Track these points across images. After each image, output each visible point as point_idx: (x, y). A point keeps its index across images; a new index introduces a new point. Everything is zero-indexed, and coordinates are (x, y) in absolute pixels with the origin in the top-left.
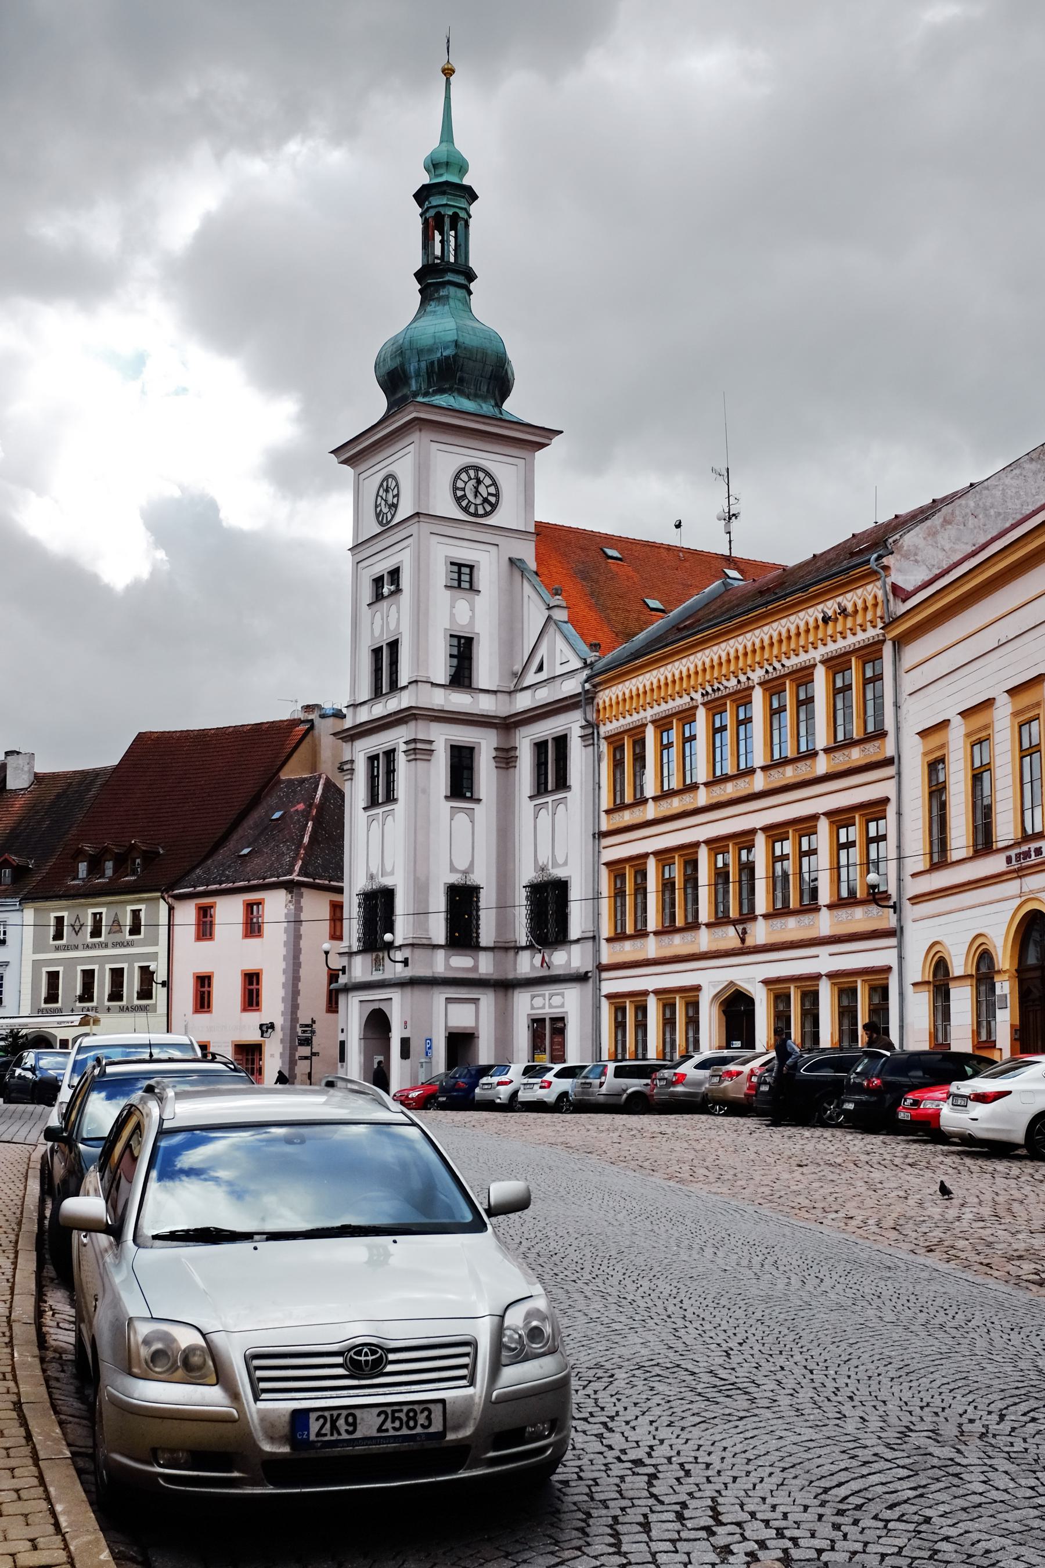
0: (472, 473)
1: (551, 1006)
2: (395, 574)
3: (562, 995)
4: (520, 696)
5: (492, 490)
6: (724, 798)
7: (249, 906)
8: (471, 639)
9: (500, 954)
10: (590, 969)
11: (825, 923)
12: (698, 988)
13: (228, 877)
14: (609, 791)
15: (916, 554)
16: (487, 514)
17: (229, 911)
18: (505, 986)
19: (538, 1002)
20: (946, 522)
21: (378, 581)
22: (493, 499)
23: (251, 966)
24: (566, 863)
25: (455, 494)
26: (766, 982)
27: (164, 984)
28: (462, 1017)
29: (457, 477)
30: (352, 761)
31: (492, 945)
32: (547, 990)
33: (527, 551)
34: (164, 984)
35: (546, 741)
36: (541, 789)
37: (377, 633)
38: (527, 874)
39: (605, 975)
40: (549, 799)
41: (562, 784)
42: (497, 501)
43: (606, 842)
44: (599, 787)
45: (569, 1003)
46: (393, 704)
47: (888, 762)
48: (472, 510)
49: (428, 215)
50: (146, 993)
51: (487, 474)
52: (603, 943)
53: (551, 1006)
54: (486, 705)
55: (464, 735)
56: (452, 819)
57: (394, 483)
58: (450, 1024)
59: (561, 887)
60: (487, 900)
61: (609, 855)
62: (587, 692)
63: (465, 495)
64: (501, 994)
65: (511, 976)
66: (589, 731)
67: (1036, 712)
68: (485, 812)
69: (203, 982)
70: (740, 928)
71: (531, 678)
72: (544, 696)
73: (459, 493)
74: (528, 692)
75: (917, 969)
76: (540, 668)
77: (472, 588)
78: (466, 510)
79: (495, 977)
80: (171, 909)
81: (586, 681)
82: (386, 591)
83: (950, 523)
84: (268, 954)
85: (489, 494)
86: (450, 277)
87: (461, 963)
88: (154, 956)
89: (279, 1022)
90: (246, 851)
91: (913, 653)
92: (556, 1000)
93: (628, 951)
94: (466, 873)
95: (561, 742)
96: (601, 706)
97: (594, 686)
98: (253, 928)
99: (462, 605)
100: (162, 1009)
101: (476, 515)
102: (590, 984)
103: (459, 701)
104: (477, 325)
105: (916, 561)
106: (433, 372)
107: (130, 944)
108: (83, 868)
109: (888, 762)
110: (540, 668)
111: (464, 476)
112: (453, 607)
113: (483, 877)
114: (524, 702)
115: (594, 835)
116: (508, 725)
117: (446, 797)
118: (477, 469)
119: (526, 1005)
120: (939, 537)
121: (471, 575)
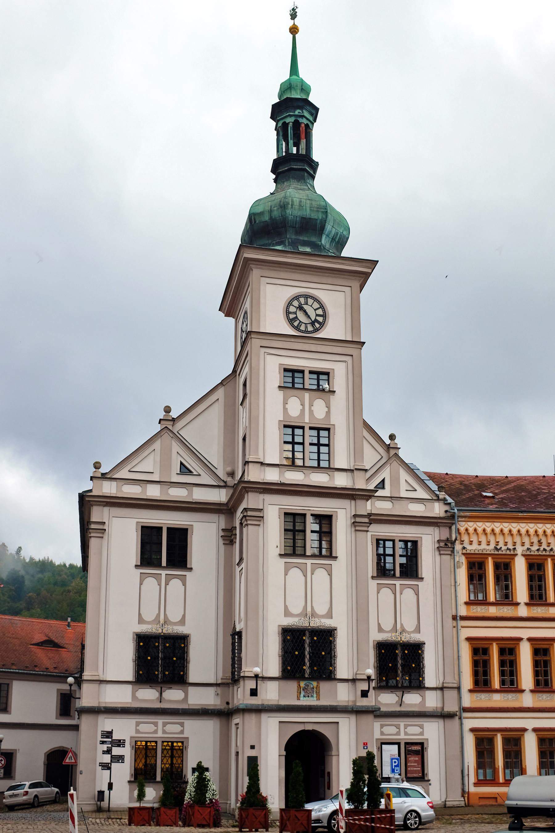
0: (302, 300)
5: (320, 312)
16: (316, 330)
22: (320, 319)
48: (303, 328)
51: (315, 299)
63: (296, 317)
85: (317, 315)
101: (306, 331)
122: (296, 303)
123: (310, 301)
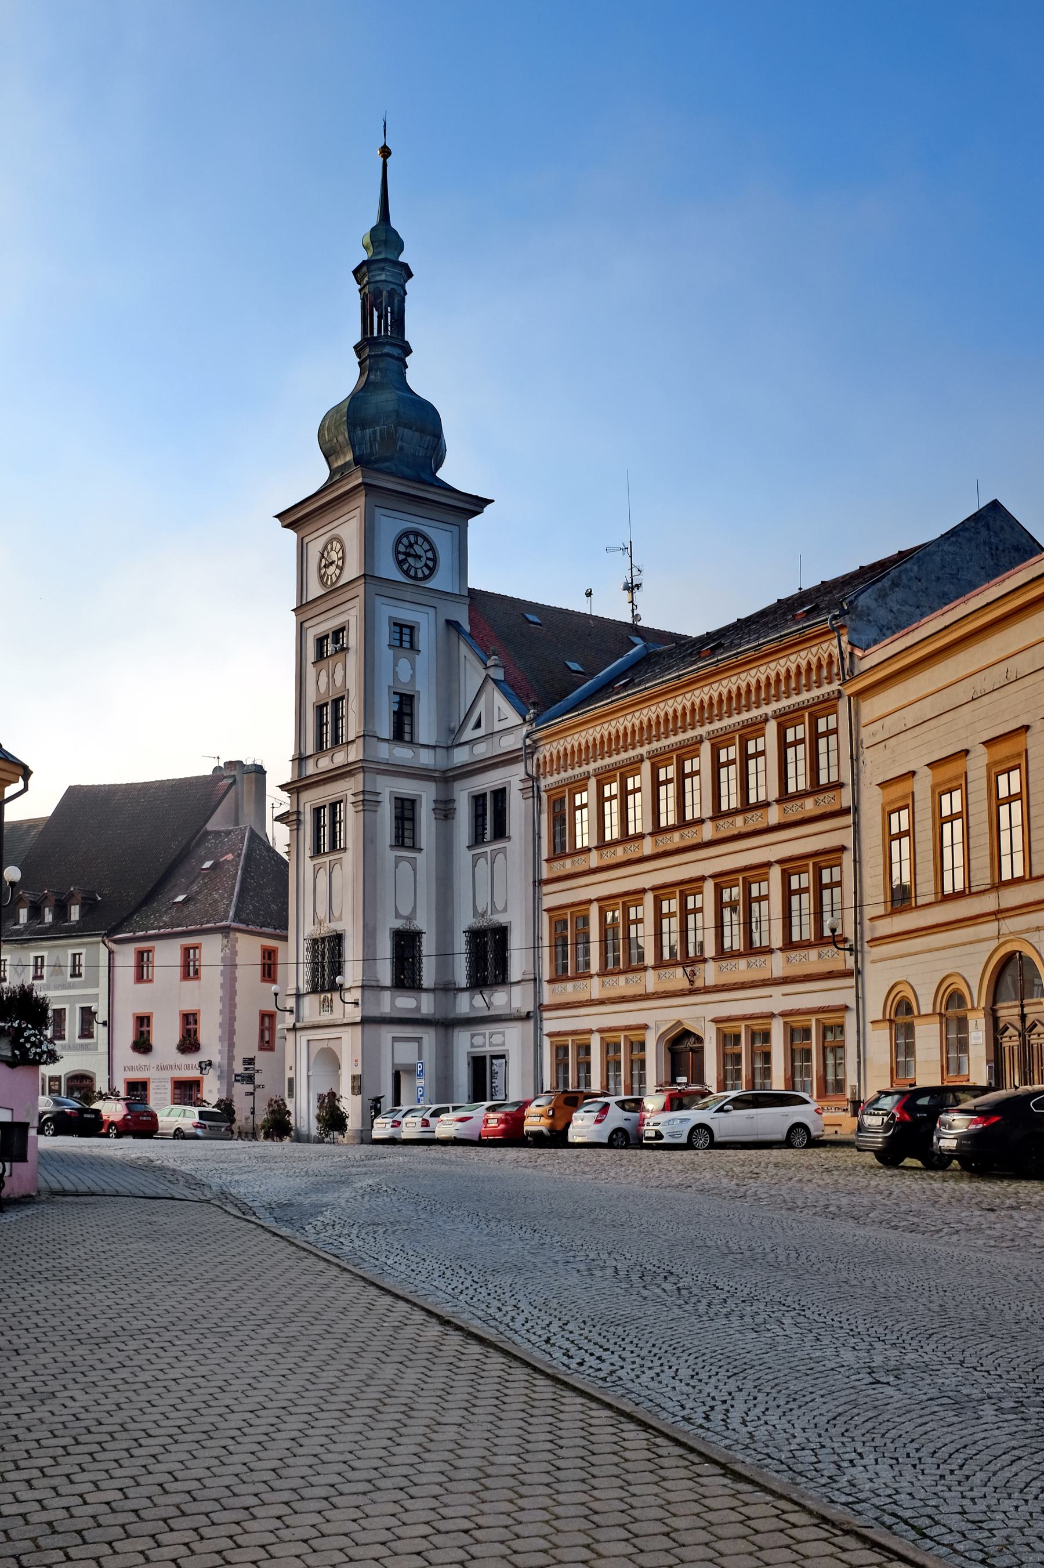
0: (412, 538)
1: (491, 1045)
2: (339, 633)
3: (503, 1034)
4: (456, 750)
5: (430, 555)
6: (670, 847)
7: (186, 950)
8: (411, 698)
9: (439, 994)
10: (531, 1009)
11: (778, 965)
12: (645, 1027)
13: (165, 922)
14: (549, 841)
15: (868, 615)
16: (426, 578)
17: (167, 955)
18: (446, 1024)
19: (478, 1040)
20: (895, 584)
21: (320, 641)
22: (430, 564)
23: (188, 1008)
24: (505, 910)
25: (397, 557)
26: (715, 1021)
27: (104, 1024)
28: (406, 1054)
29: (399, 541)
30: (298, 813)
31: (432, 986)
32: (487, 1029)
33: (462, 615)
34: (104, 1024)
35: (485, 794)
36: (478, 839)
37: (323, 689)
38: (465, 920)
39: (546, 1015)
40: (488, 849)
41: (500, 832)
42: (435, 565)
43: (546, 889)
44: (540, 838)
45: (512, 1040)
46: (340, 758)
47: (845, 812)
48: (412, 573)
49: (366, 290)
50: (86, 1033)
51: (426, 539)
52: (545, 985)
53: (491, 1045)
54: (426, 758)
55: (408, 788)
56: (396, 867)
57: (339, 546)
58: (396, 1062)
59: (501, 933)
60: (428, 946)
61: (548, 902)
62: (527, 747)
64: (441, 1031)
65: (452, 1016)
66: (530, 784)
67: (1017, 763)
68: (425, 859)
69: (143, 1021)
70: (688, 969)
71: (469, 734)
72: (481, 750)
73: (401, 557)
74: (466, 748)
75: (874, 1009)
76: (478, 725)
77: (413, 647)
78: (406, 573)
79: (437, 1017)
80: (111, 953)
81: (528, 736)
82: (330, 648)
83: (898, 585)
84: (205, 997)
85: (427, 559)
86: (387, 350)
87: (406, 1002)
88: (95, 997)
89: (216, 1059)
90: (180, 898)
91: (872, 707)
92: (497, 1039)
93: (569, 991)
94: (409, 919)
95: (500, 795)
96: (541, 761)
97: (535, 742)
98: (189, 970)
99: (404, 664)
100: (103, 1047)
101: (415, 578)
102: (530, 1024)
103: (403, 754)
104: (413, 397)
105: (869, 621)
106: (375, 440)
107: (70, 986)
108: (23, 914)
109: (845, 812)
110: (478, 725)
111: (405, 541)
112: (395, 665)
113: (424, 922)
114: (461, 756)
115: (534, 882)
116: (447, 778)
117: (391, 846)
118: (417, 534)
119: (465, 1043)
120: (888, 599)
121: (411, 635)
122: (405, 541)
123: (420, 540)
